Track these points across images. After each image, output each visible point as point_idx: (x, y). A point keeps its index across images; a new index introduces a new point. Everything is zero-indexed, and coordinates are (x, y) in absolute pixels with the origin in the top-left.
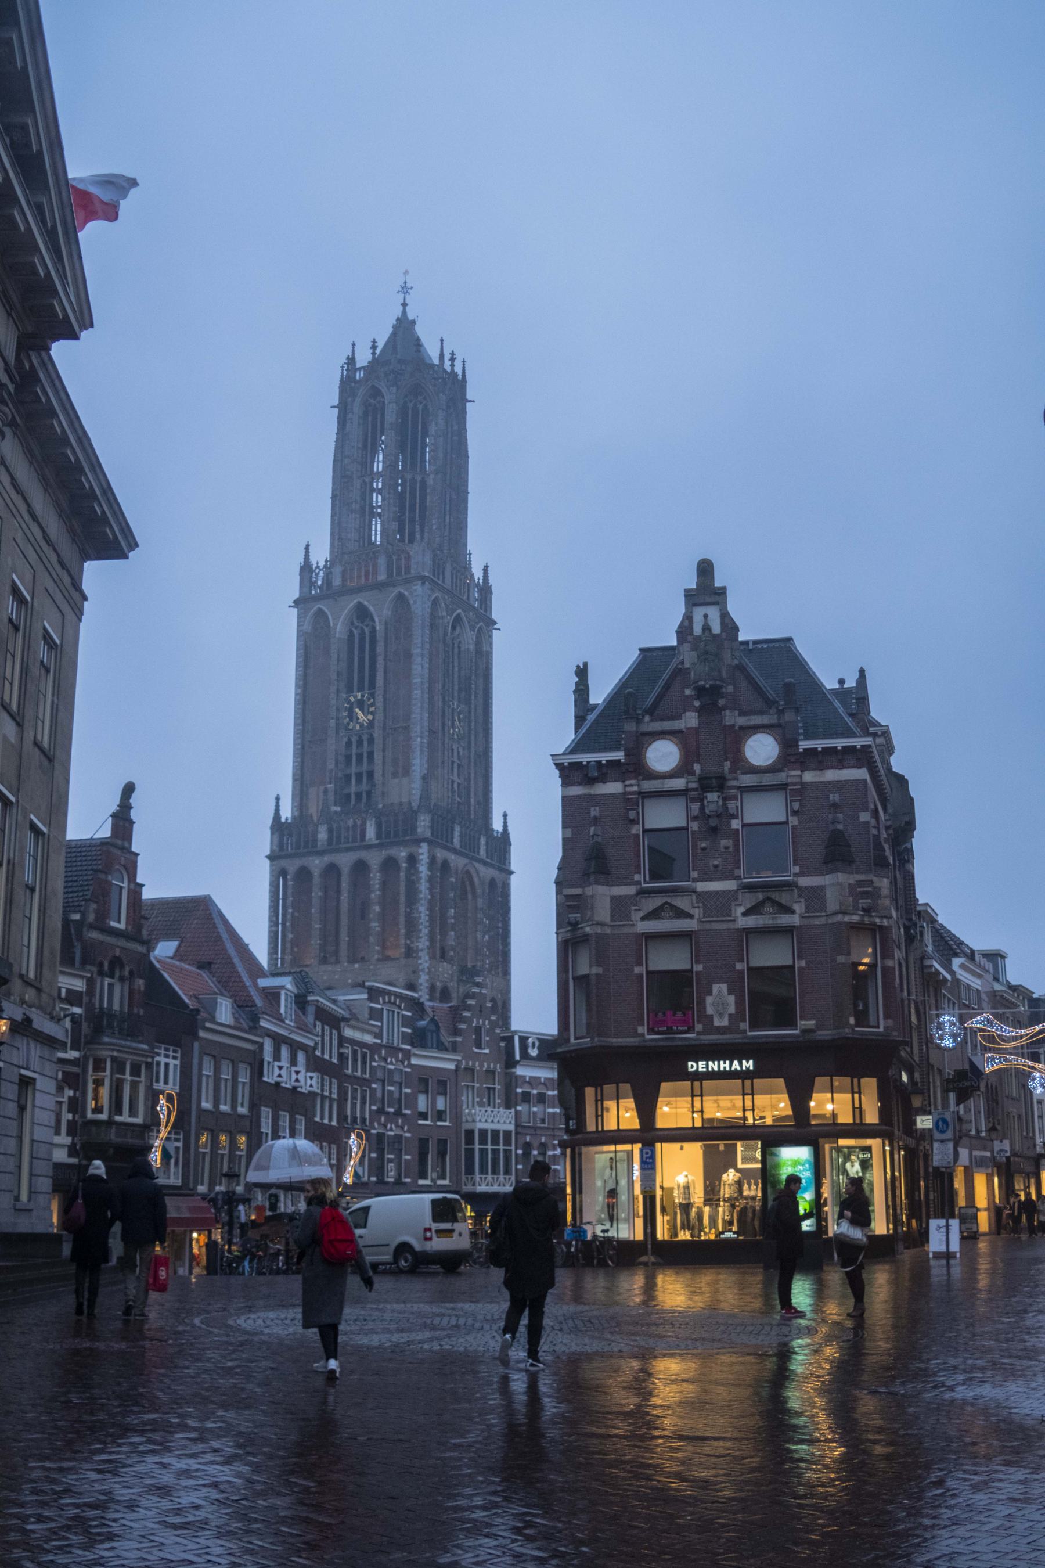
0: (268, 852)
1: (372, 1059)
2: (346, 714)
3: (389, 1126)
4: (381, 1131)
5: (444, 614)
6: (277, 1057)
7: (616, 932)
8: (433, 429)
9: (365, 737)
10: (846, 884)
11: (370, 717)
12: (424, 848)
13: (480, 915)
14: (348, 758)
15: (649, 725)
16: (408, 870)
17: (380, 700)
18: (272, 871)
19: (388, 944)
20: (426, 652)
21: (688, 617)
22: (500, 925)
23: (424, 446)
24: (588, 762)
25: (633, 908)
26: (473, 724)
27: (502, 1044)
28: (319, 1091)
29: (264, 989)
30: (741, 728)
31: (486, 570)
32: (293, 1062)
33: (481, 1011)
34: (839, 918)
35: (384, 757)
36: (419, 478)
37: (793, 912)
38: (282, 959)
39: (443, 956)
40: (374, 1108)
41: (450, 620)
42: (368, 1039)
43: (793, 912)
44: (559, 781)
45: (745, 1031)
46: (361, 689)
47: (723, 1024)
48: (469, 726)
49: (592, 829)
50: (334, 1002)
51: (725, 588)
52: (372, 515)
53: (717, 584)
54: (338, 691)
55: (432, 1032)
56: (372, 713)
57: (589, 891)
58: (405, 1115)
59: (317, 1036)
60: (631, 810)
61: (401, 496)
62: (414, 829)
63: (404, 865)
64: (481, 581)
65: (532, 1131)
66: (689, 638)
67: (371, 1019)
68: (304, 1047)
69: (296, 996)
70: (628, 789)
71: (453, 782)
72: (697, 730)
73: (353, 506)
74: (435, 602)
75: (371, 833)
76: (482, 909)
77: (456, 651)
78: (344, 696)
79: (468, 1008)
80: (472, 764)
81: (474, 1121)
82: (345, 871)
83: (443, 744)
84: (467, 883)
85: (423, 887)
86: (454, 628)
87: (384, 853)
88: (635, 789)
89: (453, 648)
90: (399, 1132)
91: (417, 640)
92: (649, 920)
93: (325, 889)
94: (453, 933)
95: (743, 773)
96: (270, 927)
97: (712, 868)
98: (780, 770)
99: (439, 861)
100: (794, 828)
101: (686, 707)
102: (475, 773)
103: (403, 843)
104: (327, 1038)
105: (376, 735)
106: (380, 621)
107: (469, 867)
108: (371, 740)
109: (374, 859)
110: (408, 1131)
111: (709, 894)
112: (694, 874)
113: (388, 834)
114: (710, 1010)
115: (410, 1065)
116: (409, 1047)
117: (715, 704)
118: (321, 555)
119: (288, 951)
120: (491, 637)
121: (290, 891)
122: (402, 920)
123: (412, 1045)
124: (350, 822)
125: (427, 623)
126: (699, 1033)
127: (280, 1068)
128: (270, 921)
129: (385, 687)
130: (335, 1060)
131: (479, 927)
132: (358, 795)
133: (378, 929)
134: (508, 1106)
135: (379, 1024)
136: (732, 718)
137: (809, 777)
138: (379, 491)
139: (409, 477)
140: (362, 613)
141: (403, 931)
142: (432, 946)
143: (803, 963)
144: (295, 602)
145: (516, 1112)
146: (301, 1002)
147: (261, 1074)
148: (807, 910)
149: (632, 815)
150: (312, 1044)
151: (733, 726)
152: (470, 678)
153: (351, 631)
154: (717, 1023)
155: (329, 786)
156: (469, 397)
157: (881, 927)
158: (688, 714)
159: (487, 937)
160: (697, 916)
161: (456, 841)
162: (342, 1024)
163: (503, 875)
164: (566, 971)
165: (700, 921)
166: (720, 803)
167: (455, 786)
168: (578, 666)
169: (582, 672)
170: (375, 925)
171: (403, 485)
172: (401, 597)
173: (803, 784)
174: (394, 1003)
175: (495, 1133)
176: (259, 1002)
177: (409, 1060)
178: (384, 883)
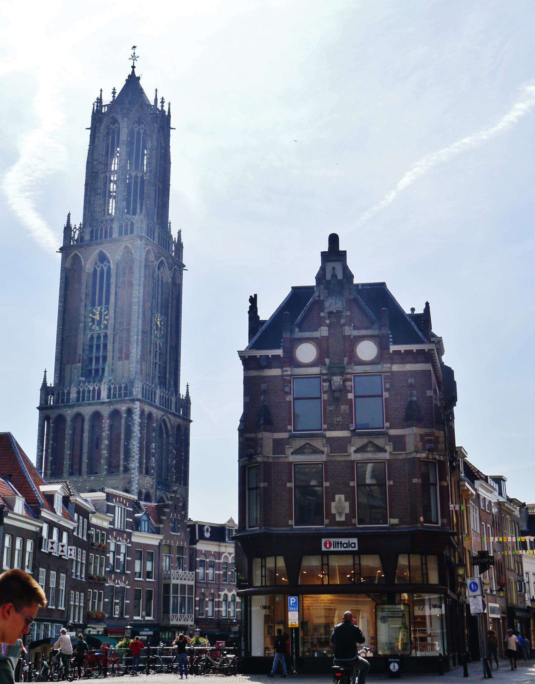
0: (38, 405)
1: (108, 538)
2: (90, 320)
3: (117, 581)
4: (112, 584)
5: (154, 259)
6: (50, 536)
7: (277, 461)
8: (149, 145)
9: (102, 335)
10: (418, 435)
11: (106, 322)
12: (137, 404)
13: (171, 447)
14: (91, 347)
15: (298, 334)
16: (127, 418)
17: (112, 311)
18: (40, 417)
19: (113, 465)
20: (142, 283)
21: (323, 269)
22: (183, 454)
23: (143, 155)
24: (260, 356)
25: (287, 446)
26: (169, 328)
27: (188, 530)
28: (75, 558)
29: (43, 492)
30: (355, 337)
31: (179, 233)
32: (60, 539)
33: (175, 508)
34: (414, 455)
35: (113, 347)
36: (139, 175)
37: (385, 451)
38: (45, 473)
39: (147, 473)
40: (108, 569)
41: (157, 263)
42: (106, 525)
43: (385, 451)
44: (242, 367)
45: (355, 525)
46: (100, 304)
47: (341, 520)
48: (167, 329)
49: (262, 397)
50: (86, 501)
51: (345, 252)
52: (110, 196)
53: (341, 249)
54: (86, 306)
55: (145, 521)
56: (106, 320)
57: (260, 435)
58: (127, 574)
59: (76, 522)
60: (287, 386)
61: (129, 186)
62: (131, 393)
63: (124, 415)
64: (176, 240)
65: (205, 586)
66: (324, 281)
67: (107, 512)
68: (67, 530)
69: (63, 497)
70: (285, 373)
71: (156, 363)
72: (327, 337)
73: (99, 190)
74: (148, 252)
75: (104, 395)
76: (172, 444)
77: (160, 283)
78: (90, 308)
79: (167, 506)
80: (168, 353)
81: (169, 578)
82: (87, 418)
83: (151, 340)
84: (163, 427)
85: (136, 429)
86: (159, 268)
87: (112, 407)
88: (289, 373)
89: (158, 280)
90: (122, 585)
91: (136, 275)
92: (296, 454)
93: (74, 429)
94: (154, 458)
95: (356, 365)
96: (38, 452)
97: (335, 423)
98: (378, 363)
99: (146, 413)
100: (386, 399)
101: (320, 323)
102: (170, 358)
103: (123, 401)
104: (81, 524)
105: (109, 334)
106: (114, 263)
107: (164, 417)
108: (106, 336)
109: (106, 411)
110: (128, 585)
111: (333, 439)
112: (325, 426)
113: (115, 397)
114: (333, 511)
115: (131, 542)
116: (130, 531)
117: (338, 322)
118: (77, 221)
119: (49, 468)
120: (181, 274)
121: (51, 430)
122: (122, 449)
123: (132, 529)
124: (91, 389)
125: (143, 264)
126: (327, 525)
127: (53, 543)
128: (38, 448)
129: (116, 303)
130: (85, 539)
131: (170, 455)
132: (97, 371)
133: (106, 455)
134: (191, 570)
135: (113, 515)
136: (348, 331)
137: (396, 368)
138: (115, 182)
139: (133, 174)
140: (103, 258)
141: (122, 457)
142: (140, 467)
143: (391, 483)
144: (60, 249)
145: (196, 572)
146: (66, 501)
147: (41, 547)
148: (394, 450)
149: (287, 389)
150: (72, 528)
151: (350, 336)
152: (168, 300)
153: (95, 269)
154: (338, 519)
155: (78, 364)
156: (172, 126)
157: (439, 461)
158: (322, 327)
159: (174, 461)
160: (326, 452)
161: (157, 400)
162: (90, 515)
163: (185, 423)
164: (245, 485)
165: (327, 455)
166: (341, 383)
167: (157, 366)
168: (251, 296)
169: (253, 300)
170: (105, 452)
171: (130, 178)
172: (126, 247)
173: (391, 372)
174: (122, 503)
175: (183, 586)
176: (41, 500)
177: (130, 539)
178: (111, 426)
